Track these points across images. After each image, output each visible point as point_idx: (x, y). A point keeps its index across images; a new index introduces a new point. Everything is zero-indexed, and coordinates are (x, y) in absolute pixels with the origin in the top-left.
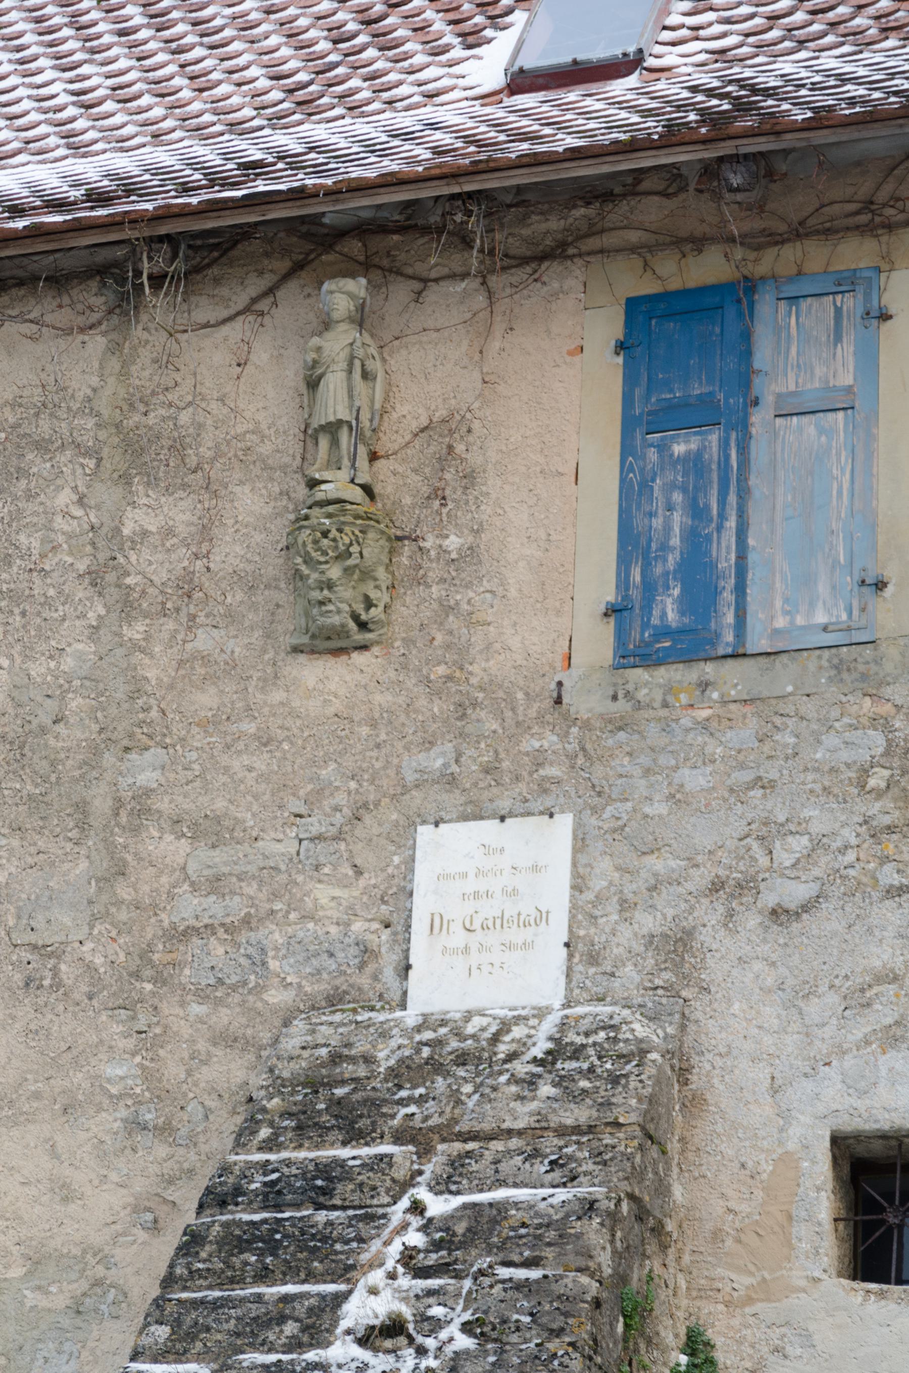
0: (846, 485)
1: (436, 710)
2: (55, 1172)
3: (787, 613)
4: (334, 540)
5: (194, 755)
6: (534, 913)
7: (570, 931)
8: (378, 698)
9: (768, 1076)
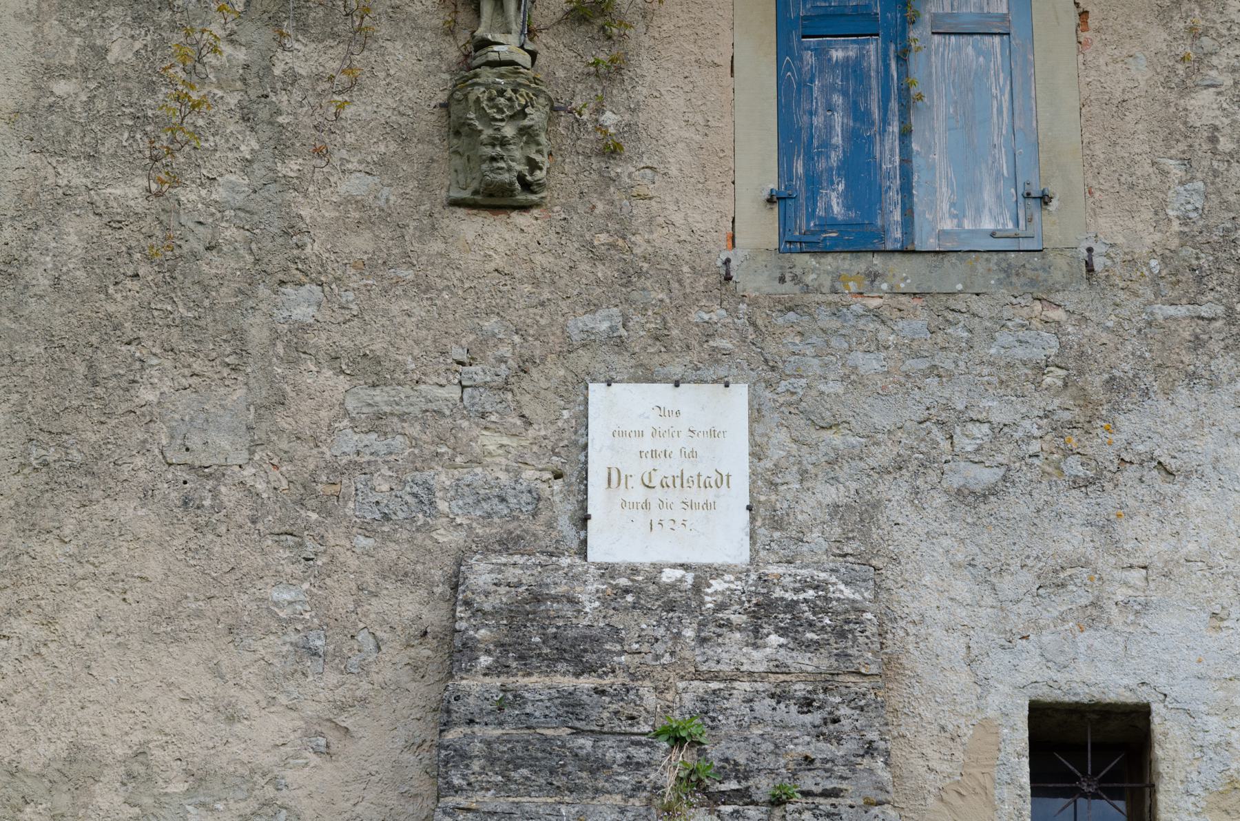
0: (1006, 105)
1: (600, 275)
2: (218, 690)
3: (955, 216)
4: (510, 99)
5: (351, 295)
6: (714, 476)
7: (751, 496)
8: (538, 258)
9: (964, 646)
